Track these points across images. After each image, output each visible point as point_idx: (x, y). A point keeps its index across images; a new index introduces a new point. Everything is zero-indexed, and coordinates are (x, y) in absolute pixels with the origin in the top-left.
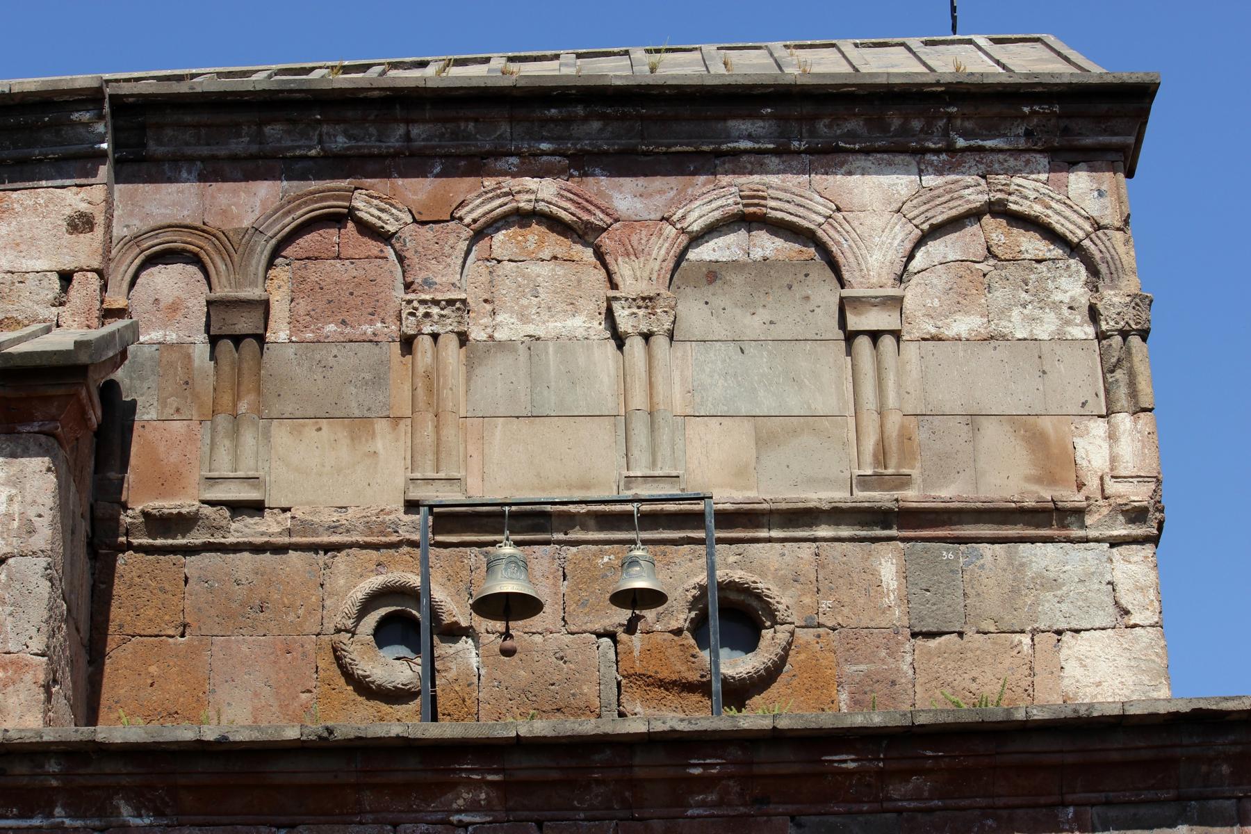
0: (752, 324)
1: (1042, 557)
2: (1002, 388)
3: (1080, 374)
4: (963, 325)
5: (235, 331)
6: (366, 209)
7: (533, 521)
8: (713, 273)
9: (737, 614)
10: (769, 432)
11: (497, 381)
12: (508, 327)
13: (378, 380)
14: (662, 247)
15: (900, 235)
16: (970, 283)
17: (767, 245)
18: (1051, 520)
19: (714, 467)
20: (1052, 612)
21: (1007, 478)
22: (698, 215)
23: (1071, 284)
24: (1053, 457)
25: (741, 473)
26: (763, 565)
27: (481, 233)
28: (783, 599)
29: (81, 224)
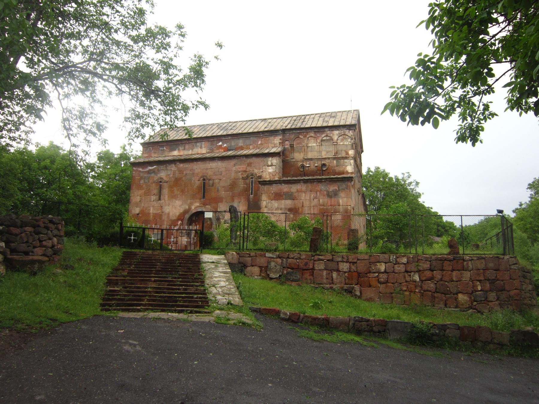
0: (327, 144)
1: (346, 161)
2: (344, 148)
3: (349, 147)
4: (341, 143)
5: (292, 146)
6: (300, 136)
7: (311, 159)
8: (324, 140)
9: (324, 165)
10: (327, 152)
11: (309, 149)
12: (310, 145)
13: (301, 149)
14: (320, 139)
15: (337, 137)
16: (342, 140)
17: (328, 138)
18: (346, 158)
19: (324, 155)
20: (346, 164)
21: (344, 155)
22: (323, 136)
23: (349, 140)
24: (347, 153)
25: (325, 155)
26: (326, 162)
27: (308, 138)
28: (327, 164)
29: (280, 139)
